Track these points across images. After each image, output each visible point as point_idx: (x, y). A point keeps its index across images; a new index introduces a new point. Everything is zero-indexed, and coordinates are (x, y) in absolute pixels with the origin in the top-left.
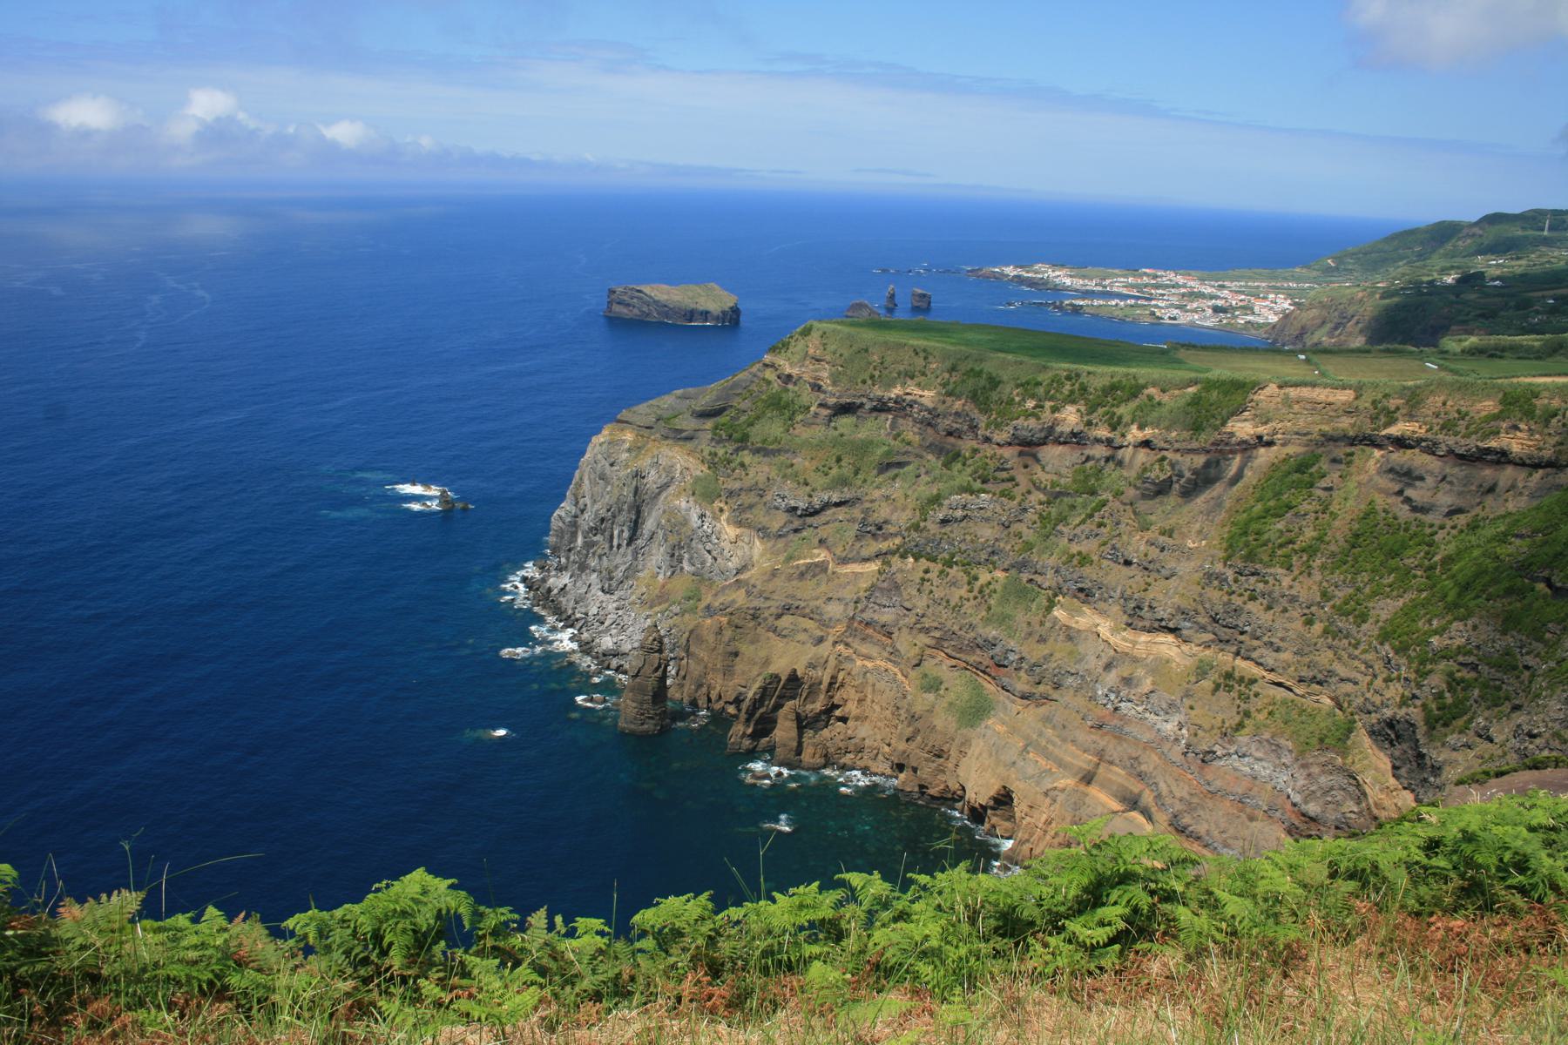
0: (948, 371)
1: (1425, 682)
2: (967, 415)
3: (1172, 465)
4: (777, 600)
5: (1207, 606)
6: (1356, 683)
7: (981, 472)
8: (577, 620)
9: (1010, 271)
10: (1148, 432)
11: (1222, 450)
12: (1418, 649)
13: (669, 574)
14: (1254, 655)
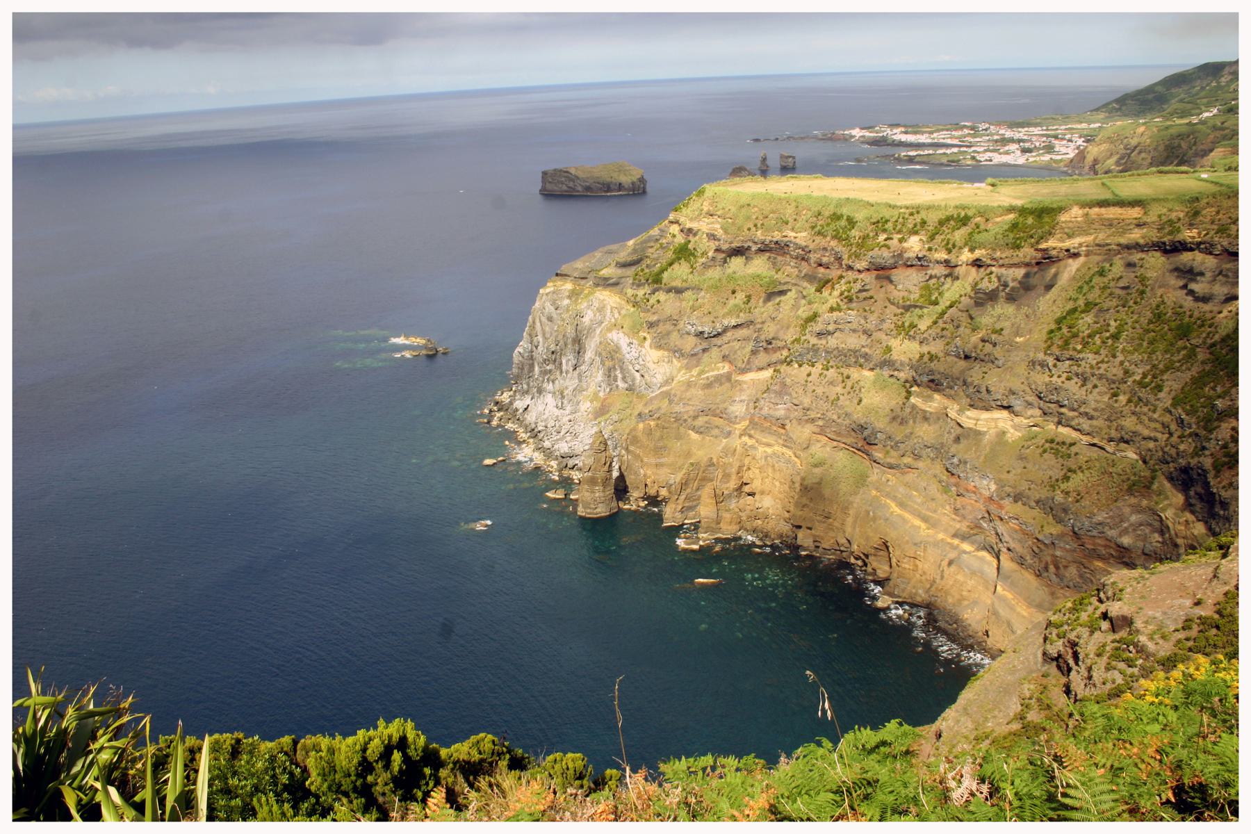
0: (815, 216)
1: (1212, 436)
2: (833, 249)
3: (999, 278)
4: (693, 405)
5: (1033, 387)
6: (1156, 440)
7: (846, 294)
8: (539, 432)
9: (857, 133)
10: (978, 253)
11: (1047, 260)
12: (1205, 410)
13: (608, 390)
14: (1073, 423)
